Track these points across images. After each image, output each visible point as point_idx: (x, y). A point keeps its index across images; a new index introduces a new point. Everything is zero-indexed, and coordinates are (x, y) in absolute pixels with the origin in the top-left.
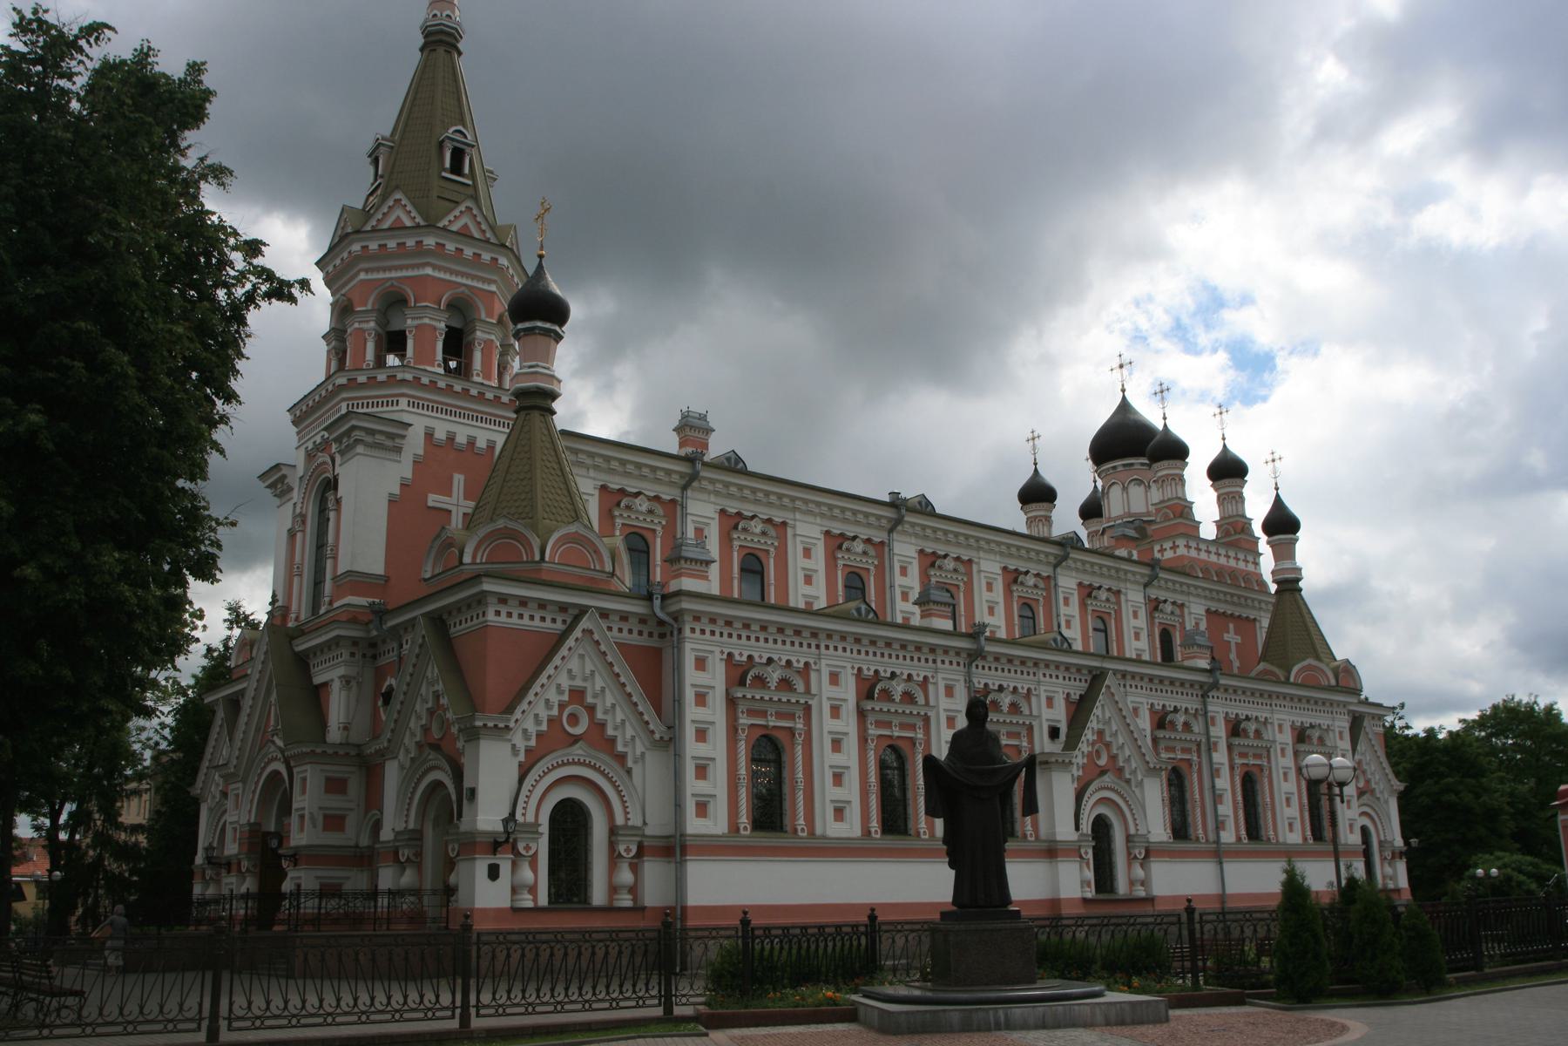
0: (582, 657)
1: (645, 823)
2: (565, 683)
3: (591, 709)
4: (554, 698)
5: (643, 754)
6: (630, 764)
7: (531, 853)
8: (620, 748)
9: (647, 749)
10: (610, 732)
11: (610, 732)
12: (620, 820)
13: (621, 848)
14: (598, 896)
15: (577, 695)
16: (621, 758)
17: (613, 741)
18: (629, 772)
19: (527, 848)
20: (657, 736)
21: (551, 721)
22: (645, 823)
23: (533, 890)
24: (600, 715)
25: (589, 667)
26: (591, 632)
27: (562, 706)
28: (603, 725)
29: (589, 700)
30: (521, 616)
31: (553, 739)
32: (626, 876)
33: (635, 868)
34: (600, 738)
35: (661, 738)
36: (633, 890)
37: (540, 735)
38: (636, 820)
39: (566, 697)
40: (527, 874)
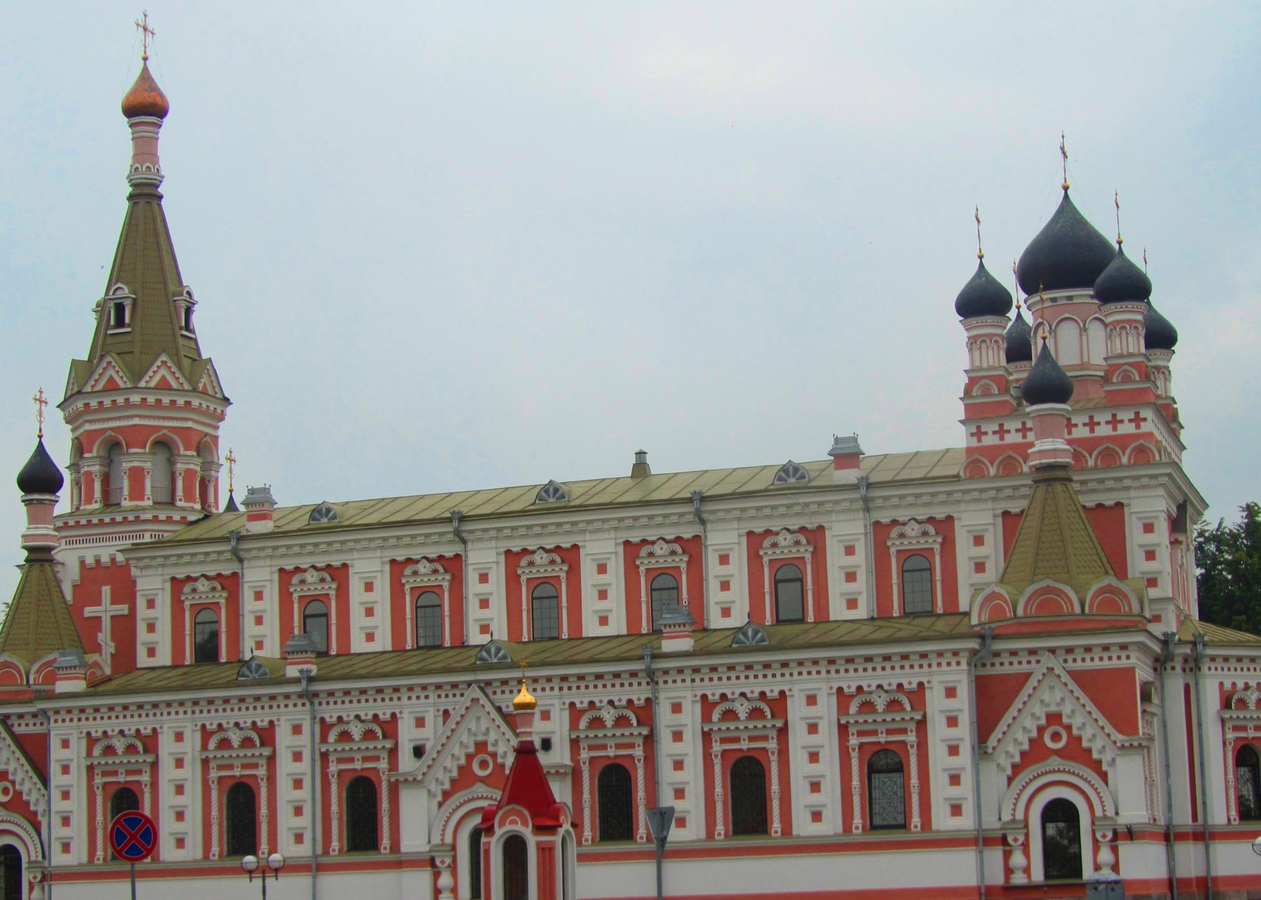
0: (1052, 688)
1: (1117, 813)
2: (1040, 712)
3: (1068, 728)
4: (1032, 725)
5: (1114, 760)
6: (1105, 768)
7: (1020, 842)
8: (1095, 756)
9: (1117, 755)
10: (1085, 744)
11: (1085, 744)
12: (1098, 813)
13: (1098, 836)
14: (1088, 873)
15: (1054, 718)
16: (1096, 766)
17: (1089, 751)
18: (1104, 776)
19: (1016, 840)
20: (1119, 744)
21: (1031, 741)
22: (1117, 813)
23: (1027, 870)
24: (1075, 732)
25: (1058, 695)
26: (1053, 669)
27: (1041, 730)
28: (1079, 739)
29: (1065, 720)
30: (1011, 663)
31: (1034, 753)
32: (1105, 855)
33: (1115, 850)
34: (1077, 752)
35: (1123, 746)
36: (1115, 868)
37: (1023, 754)
38: (1110, 812)
39: (1043, 722)
40: (1018, 859)
